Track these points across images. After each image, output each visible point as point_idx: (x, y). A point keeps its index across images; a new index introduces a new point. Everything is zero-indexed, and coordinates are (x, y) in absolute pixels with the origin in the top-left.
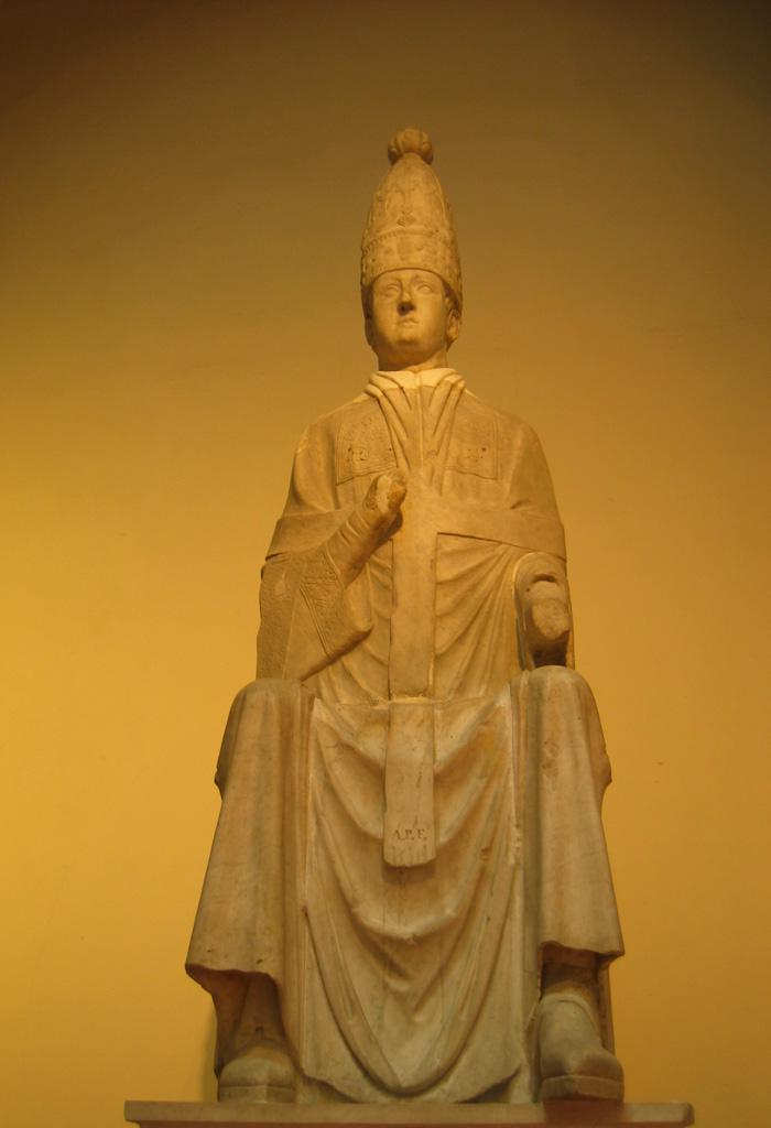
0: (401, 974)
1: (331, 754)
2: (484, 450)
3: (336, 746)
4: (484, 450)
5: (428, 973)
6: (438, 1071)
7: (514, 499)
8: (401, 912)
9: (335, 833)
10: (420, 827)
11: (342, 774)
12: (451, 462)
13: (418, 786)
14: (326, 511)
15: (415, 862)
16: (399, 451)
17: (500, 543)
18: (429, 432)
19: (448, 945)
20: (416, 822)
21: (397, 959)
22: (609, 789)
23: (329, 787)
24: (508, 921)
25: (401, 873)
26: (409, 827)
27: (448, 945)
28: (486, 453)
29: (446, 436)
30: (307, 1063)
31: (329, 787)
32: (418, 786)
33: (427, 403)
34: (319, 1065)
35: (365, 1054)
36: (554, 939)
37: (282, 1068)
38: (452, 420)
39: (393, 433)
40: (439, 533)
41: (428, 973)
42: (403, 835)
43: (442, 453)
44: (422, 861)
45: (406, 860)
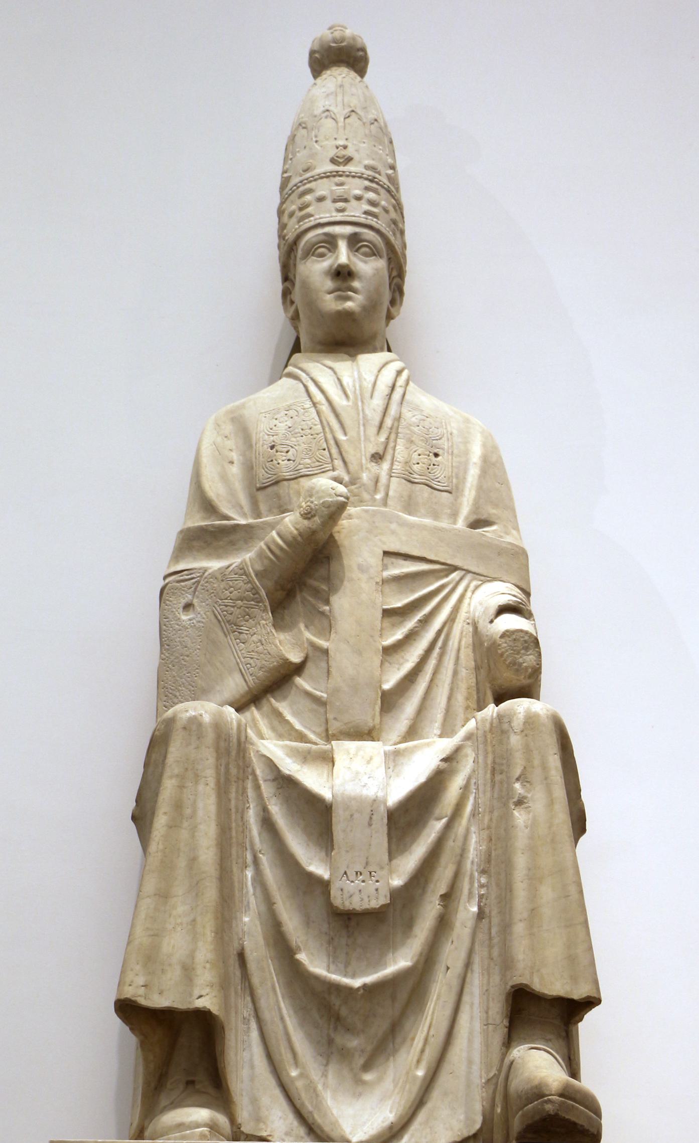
0: (349, 1030)
1: (267, 790)
2: (436, 455)
3: (274, 780)
4: (436, 455)
5: (380, 1026)
6: (391, 1127)
7: (473, 518)
8: (347, 964)
9: (271, 874)
10: (371, 868)
11: (276, 810)
12: (397, 467)
13: (370, 825)
14: (243, 522)
15: (366, 905)
16: (334, 451)
17: (455, 568)
18: (372, 430)
19: (402, 996)
20: (367, 863)
21: (344, 1012)
22: (582, 839)
23: (267, 823)
24: (469, 971)
25: (349, 919)
26: (359, 868)
27: (402, 996)
28: (439, 458)
29: (393, 436)
30: (244, 1115)
31: (267, 823)
32: (370, 825)
33: (368, 395)
34: (258, 1119)
35: (310, 1108)
36: (525, 982)
37: (222, 1120)
38: (398, 419)
39: (327, 429)
40: (386, 553)
41: (380, 1026)
42: (352, 876)
43: (388, 457)
44: (375, 904)
45: (357, 904)
